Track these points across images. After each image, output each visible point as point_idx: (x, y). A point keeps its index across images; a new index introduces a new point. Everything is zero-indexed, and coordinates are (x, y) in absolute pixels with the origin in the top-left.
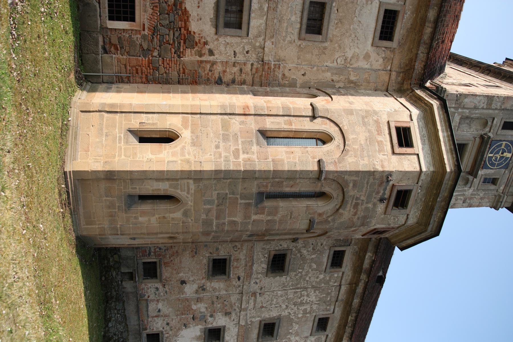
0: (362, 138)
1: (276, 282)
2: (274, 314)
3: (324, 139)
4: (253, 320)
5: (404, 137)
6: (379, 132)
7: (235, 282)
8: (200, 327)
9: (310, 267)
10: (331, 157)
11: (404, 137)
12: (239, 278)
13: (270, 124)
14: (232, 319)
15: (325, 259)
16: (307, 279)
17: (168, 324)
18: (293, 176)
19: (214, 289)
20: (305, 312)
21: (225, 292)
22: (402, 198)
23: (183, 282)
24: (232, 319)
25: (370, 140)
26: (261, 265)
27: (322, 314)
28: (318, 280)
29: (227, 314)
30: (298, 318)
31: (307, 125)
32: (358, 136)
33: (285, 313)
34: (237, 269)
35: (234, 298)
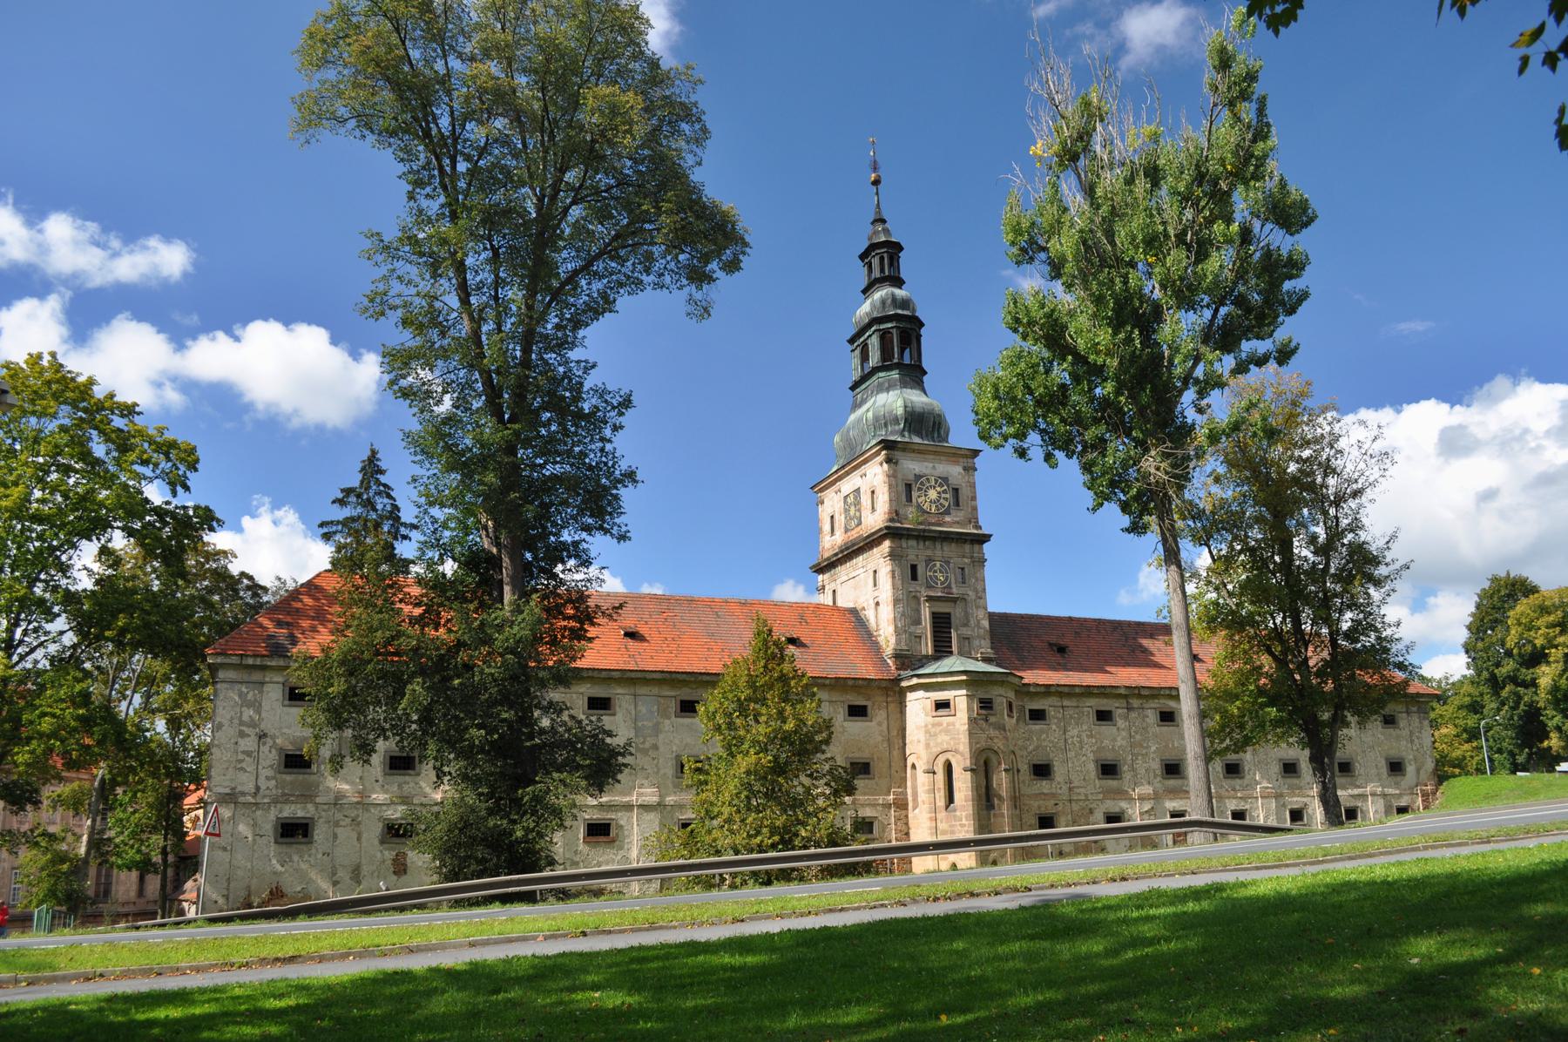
0: (947, 738)
1: (1059, 771)
2: (1092, 767)
3: (949, 768)
5: (942, 705)
6: (940, 724)
7: (1060, 808)
10: (960, 764)
11: (942, 705)
13: (941, 802)
15: (1037, 727)
18: (976, 788)
20: (1091, 736)
22: (986, 704)
25: (947, 731)
26: (1044, 786)
27: (1093, 717)
29: (1091, 811)
31: (940, 776)
32: (944, 740)
33: (1091, 756)
34: (1047, 807)
35: (1075, 807)
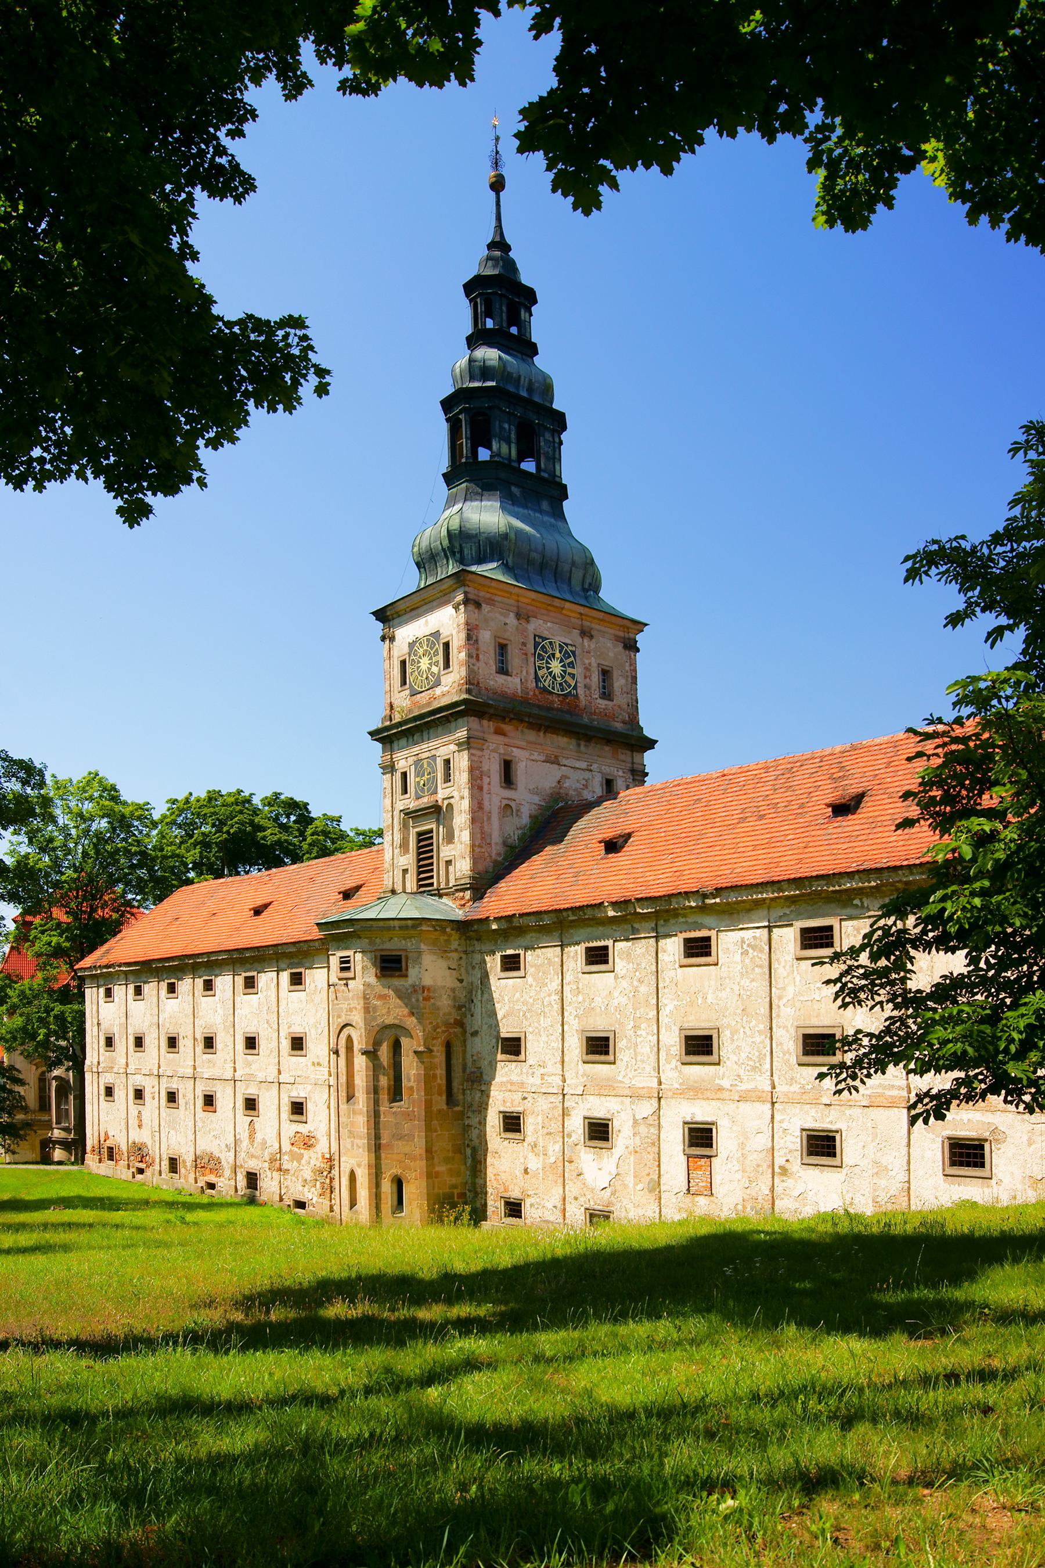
4: (581, 1072)
8: (582, 1154)
9: (518, 1000)
12: (525, 1098)
14: (574, 1105)
16: (531, 1001)
17: (576, 1199)
19: (536, 1131)
21: (540, 1117)
23: (526, 1171)
24: (574, 1105)
28: (534, 984)
30: (584, 1001)
